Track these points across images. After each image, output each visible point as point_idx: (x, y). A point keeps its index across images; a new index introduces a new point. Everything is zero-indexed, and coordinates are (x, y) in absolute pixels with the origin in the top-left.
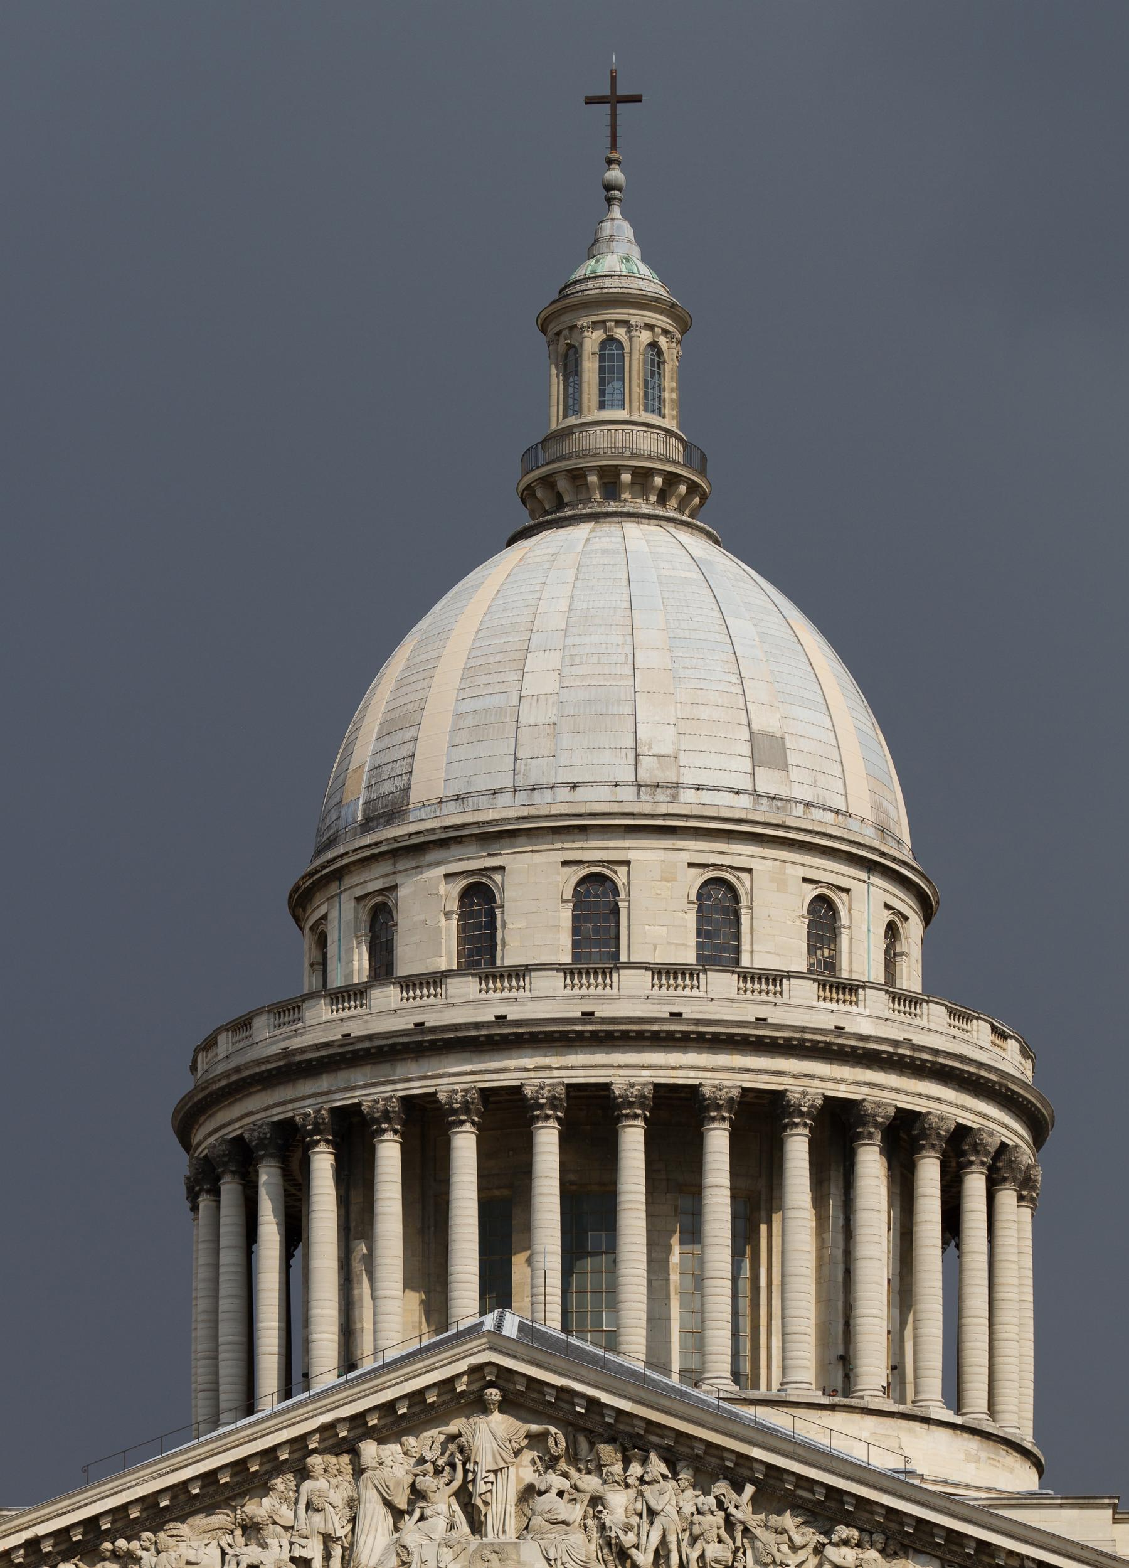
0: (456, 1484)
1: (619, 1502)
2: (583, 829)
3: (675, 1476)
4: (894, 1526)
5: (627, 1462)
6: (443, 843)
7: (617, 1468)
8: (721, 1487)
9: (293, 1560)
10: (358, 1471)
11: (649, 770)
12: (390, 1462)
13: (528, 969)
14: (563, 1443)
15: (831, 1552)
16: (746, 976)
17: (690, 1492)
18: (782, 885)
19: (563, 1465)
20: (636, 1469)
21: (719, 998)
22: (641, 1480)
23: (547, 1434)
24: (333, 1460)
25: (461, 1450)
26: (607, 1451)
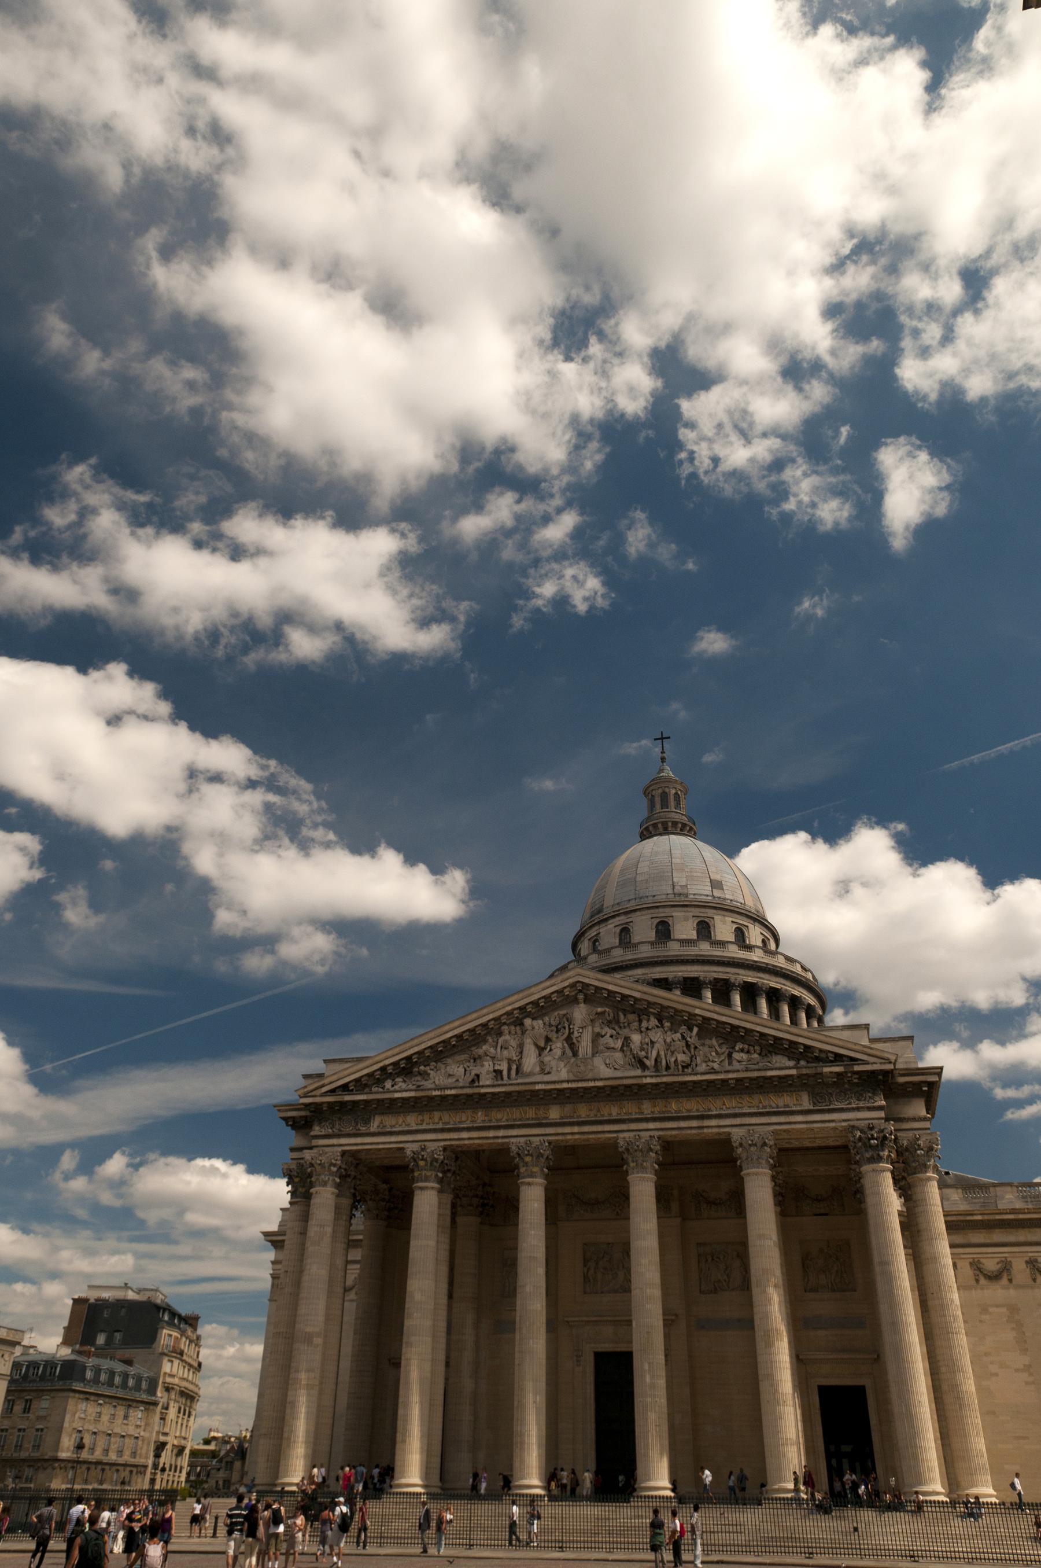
1: (636, 1038)
2: (657, 907)
4: (764, 1042)
6: (614, 917)
7: (636, 1024)
9: (495, 1071)
11: (678, 889)
12: (536, 1026)
13: (639, 943)
14: (612, 1015)
15: (736, 1056)
17: (669, 1033)
18: (724, 923)
20: (644, 1024)
21: (704, 948)
22: (647, 1029)
23: (604, 1012)
24: (513, 1028)
26: (632, 1017)
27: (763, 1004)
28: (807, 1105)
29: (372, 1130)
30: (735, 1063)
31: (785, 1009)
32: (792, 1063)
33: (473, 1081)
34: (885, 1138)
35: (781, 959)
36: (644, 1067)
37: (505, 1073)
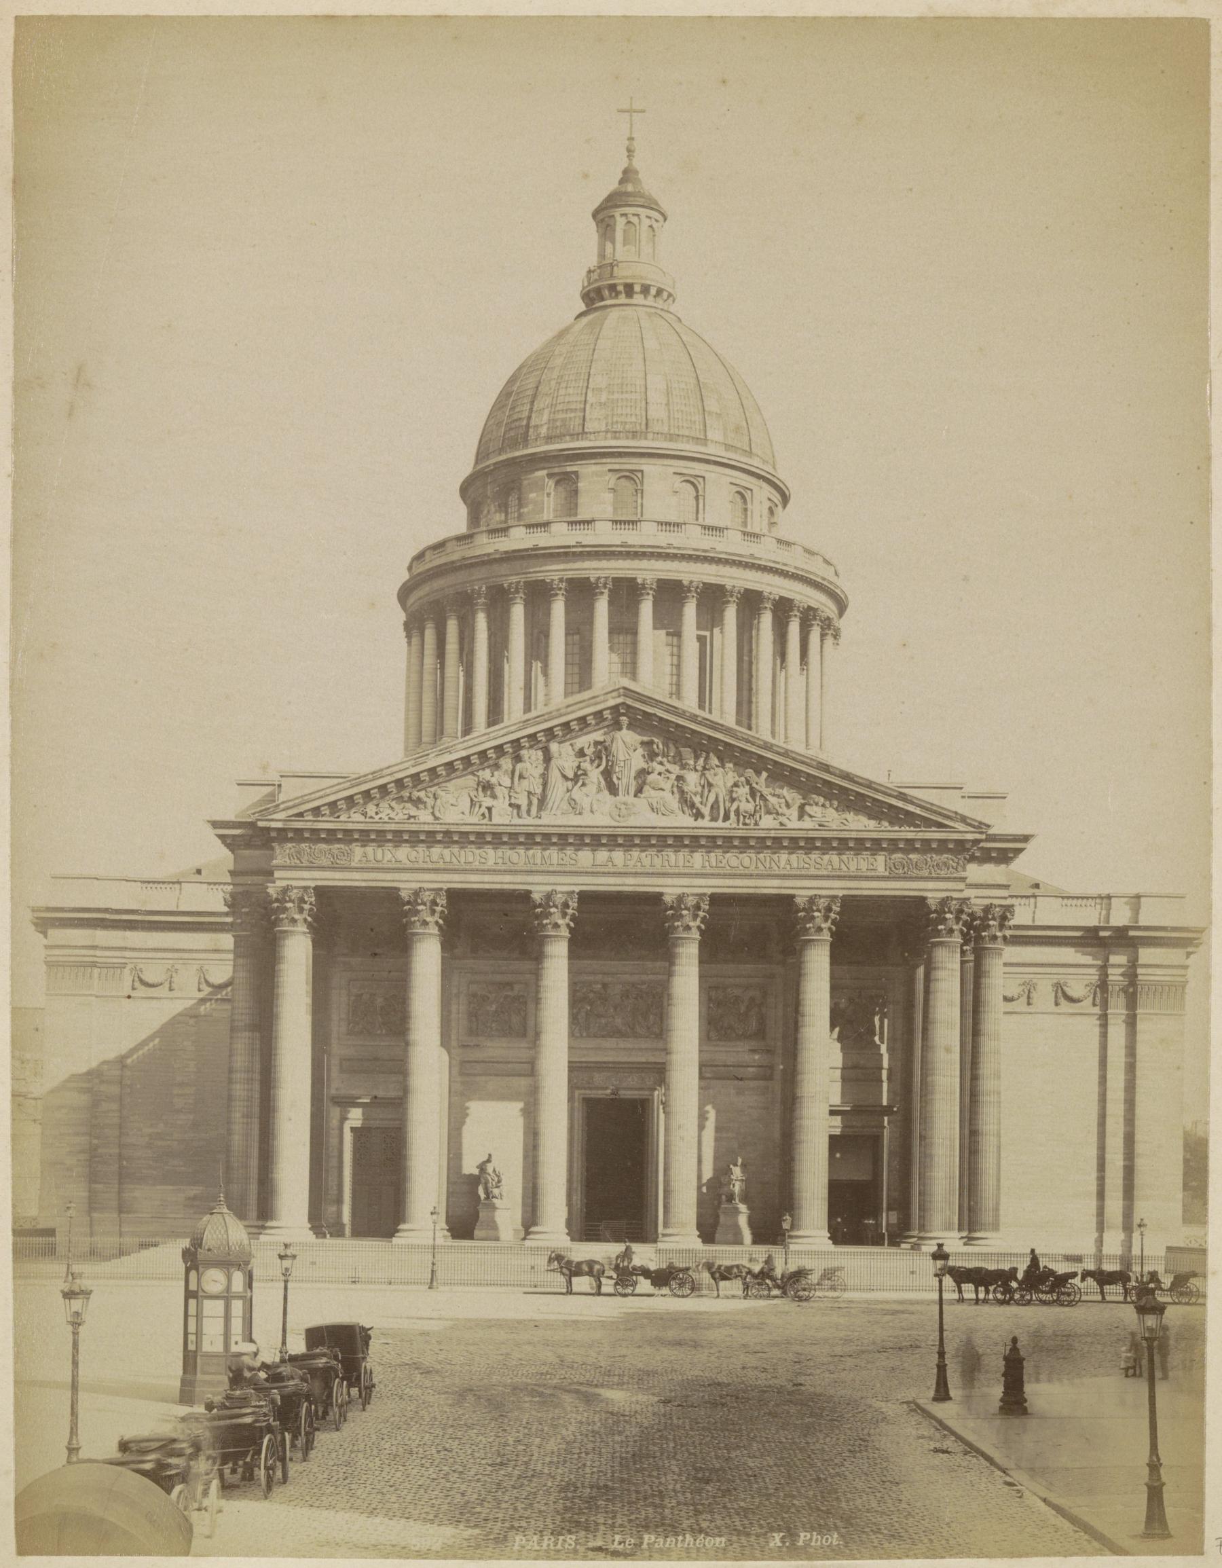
0: (602, 768)
1: (692, 780)
2: (620, 455)
3: (723, 766)
5: (697, 758)
7: (691, 762)
8: (750, 772)
10: (548, 758)
15: (807, 808)
16: (705, 527)
19: (659, 759)
20: (701, 761)
22: (704, 768)
24: (532, 752)
25: (606, 749)
27: (766, 620)
28: (881, 869)
29: (353, 864)
30: (806, 817)
31: (794, 628)
32: (872, 824)
33: (483, 815)
34: (961, 911)
35: (800, 549)
36: (698, 815)
37: (524, 808)
